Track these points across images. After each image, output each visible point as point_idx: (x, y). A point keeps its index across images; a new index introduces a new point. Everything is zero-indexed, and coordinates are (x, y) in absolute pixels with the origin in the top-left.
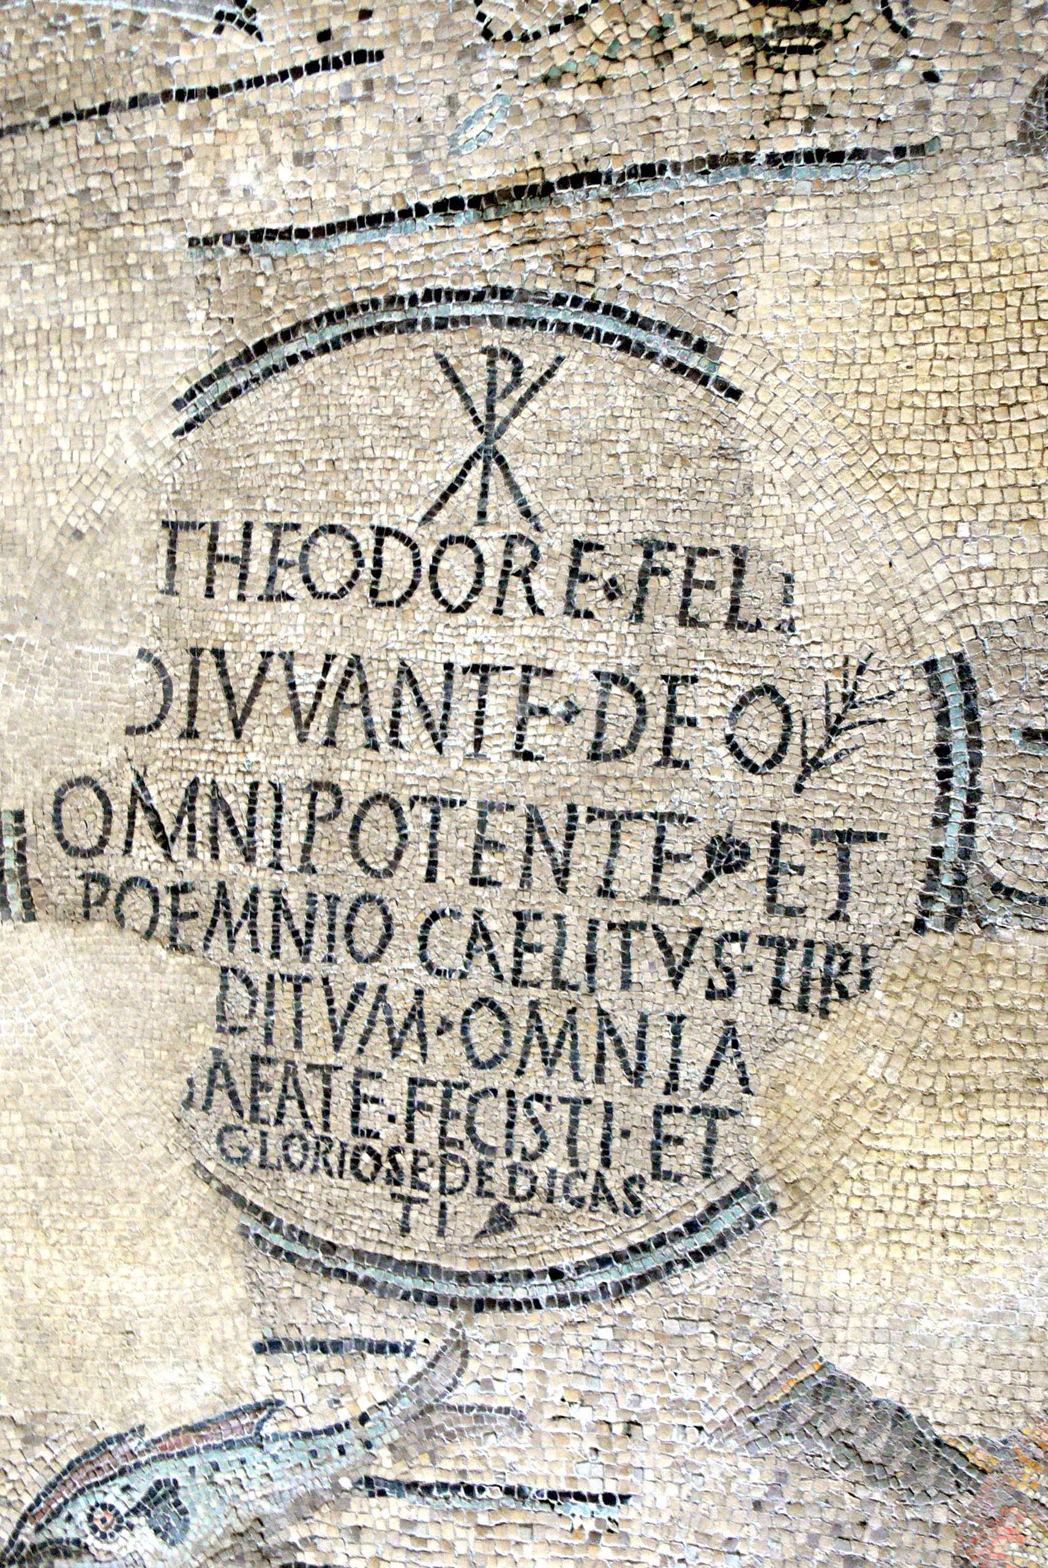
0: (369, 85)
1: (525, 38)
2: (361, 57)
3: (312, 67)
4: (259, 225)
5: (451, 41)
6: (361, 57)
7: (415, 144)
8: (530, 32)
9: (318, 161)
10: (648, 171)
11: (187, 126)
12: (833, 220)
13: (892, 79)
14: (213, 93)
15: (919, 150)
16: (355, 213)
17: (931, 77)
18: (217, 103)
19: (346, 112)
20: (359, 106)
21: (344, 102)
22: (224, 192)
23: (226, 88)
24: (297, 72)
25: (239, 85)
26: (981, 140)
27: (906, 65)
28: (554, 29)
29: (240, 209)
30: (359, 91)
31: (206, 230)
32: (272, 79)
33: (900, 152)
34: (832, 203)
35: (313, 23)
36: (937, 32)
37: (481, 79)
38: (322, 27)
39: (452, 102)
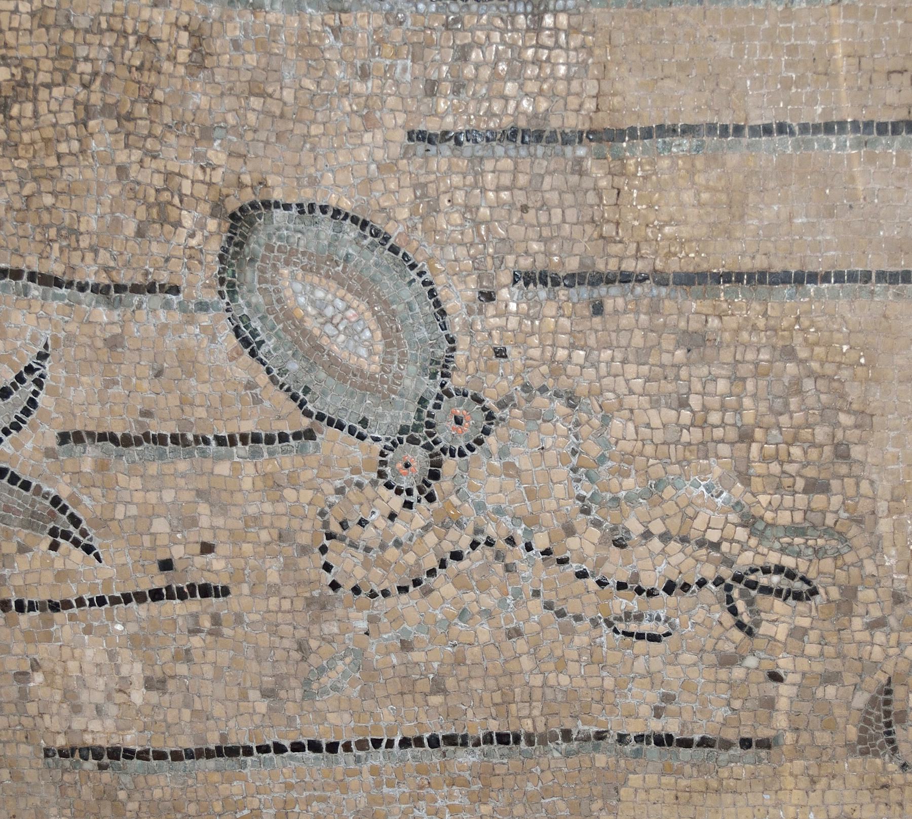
0: (216, 620)
1: (373, 595)
2: (206, 591)
3: (156, 595)
4: (115, 741)
5: (299, 584)
6: (206, 591)
7: (268, 681)
8: (377, 590)
9: (171, 685)
10: (503, 739)
11: (29, 637)
12: (682, 800)
13: (738, 673)
14: (55, 607)
15: (765, 744)
16: (213, 742)
17: (775, 677)
18: (61, 616)
19: (196, 641)
20: (209, 639)
21: (194, 632)
22: (77, 709)
23: (67, 605)
24: (140, 597)
25: (80, 602)
26: (824, 738)
27: (751, 662)
28: (403, 589)
29: (95, 725)
30: (206, 624)
31: (61, 741)
32: (115, 601)
33: (746, 743)
34: (683, 783)
35: (153, 549)
36: (781, 632)
37: (332, 628)
38: (164, 556)
39: (302, 647)
